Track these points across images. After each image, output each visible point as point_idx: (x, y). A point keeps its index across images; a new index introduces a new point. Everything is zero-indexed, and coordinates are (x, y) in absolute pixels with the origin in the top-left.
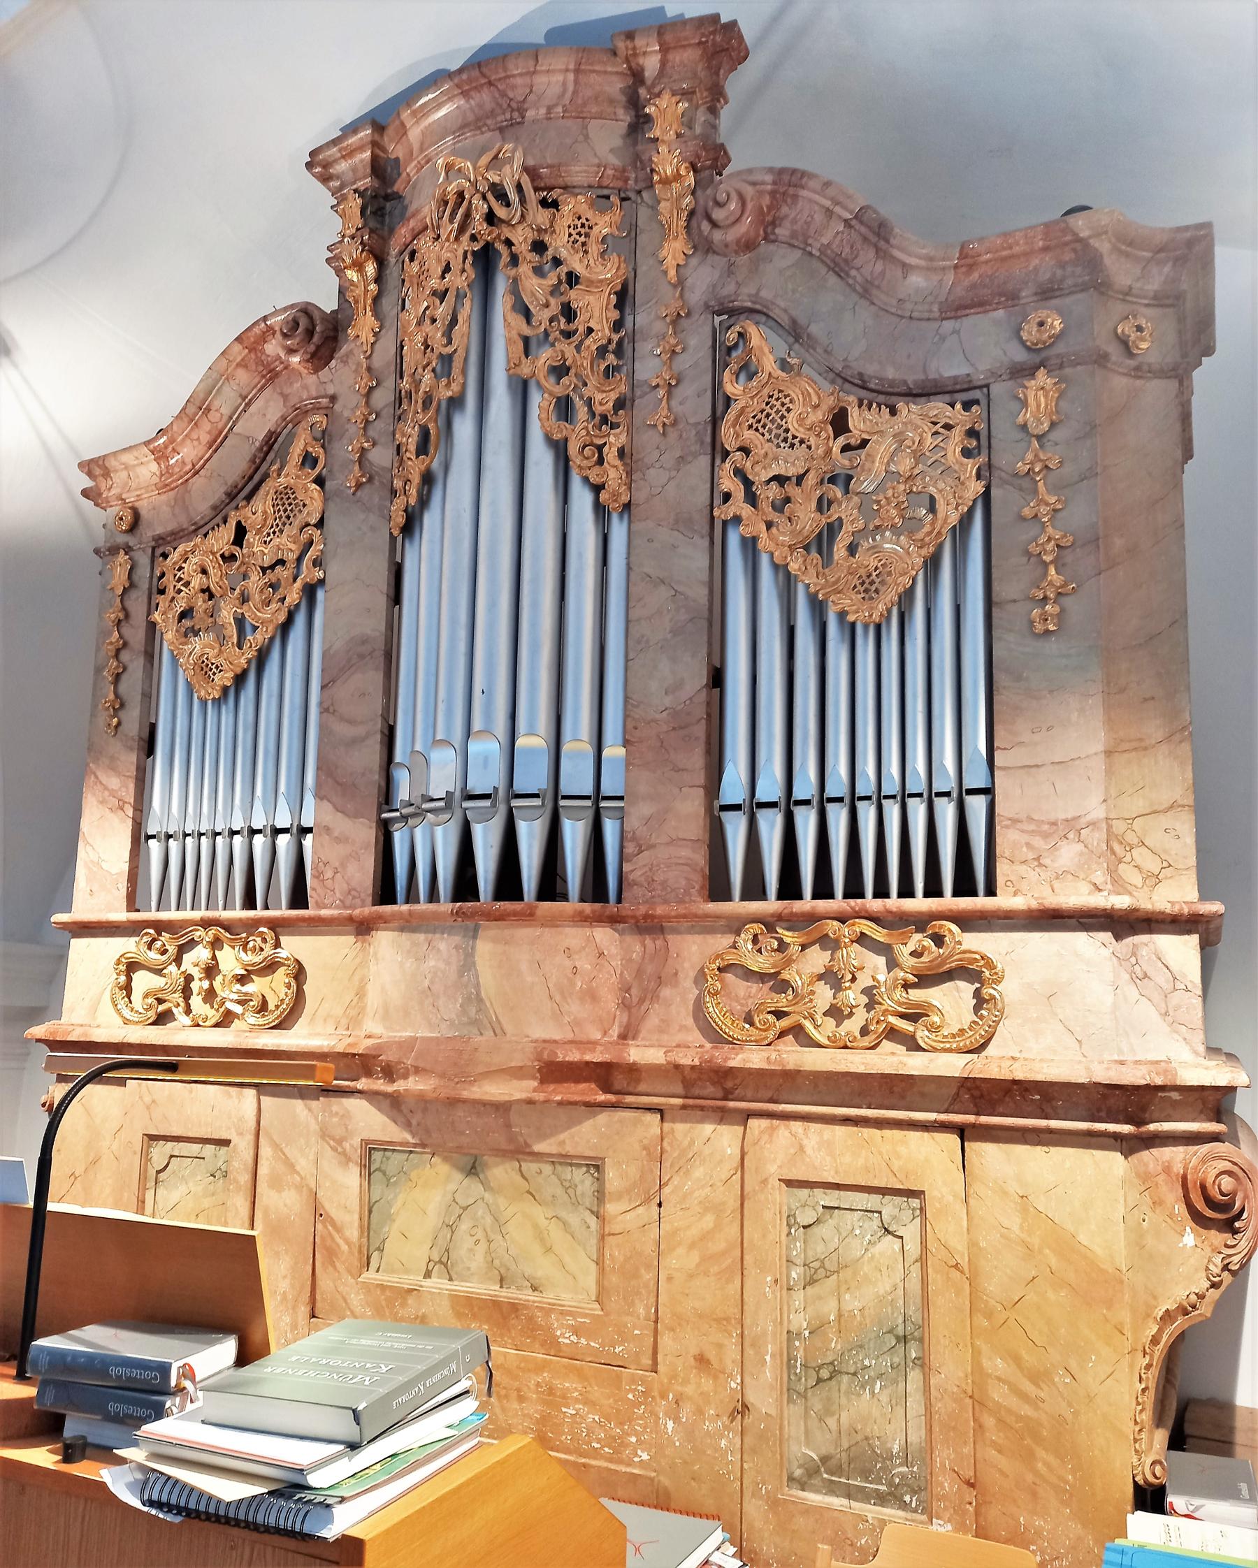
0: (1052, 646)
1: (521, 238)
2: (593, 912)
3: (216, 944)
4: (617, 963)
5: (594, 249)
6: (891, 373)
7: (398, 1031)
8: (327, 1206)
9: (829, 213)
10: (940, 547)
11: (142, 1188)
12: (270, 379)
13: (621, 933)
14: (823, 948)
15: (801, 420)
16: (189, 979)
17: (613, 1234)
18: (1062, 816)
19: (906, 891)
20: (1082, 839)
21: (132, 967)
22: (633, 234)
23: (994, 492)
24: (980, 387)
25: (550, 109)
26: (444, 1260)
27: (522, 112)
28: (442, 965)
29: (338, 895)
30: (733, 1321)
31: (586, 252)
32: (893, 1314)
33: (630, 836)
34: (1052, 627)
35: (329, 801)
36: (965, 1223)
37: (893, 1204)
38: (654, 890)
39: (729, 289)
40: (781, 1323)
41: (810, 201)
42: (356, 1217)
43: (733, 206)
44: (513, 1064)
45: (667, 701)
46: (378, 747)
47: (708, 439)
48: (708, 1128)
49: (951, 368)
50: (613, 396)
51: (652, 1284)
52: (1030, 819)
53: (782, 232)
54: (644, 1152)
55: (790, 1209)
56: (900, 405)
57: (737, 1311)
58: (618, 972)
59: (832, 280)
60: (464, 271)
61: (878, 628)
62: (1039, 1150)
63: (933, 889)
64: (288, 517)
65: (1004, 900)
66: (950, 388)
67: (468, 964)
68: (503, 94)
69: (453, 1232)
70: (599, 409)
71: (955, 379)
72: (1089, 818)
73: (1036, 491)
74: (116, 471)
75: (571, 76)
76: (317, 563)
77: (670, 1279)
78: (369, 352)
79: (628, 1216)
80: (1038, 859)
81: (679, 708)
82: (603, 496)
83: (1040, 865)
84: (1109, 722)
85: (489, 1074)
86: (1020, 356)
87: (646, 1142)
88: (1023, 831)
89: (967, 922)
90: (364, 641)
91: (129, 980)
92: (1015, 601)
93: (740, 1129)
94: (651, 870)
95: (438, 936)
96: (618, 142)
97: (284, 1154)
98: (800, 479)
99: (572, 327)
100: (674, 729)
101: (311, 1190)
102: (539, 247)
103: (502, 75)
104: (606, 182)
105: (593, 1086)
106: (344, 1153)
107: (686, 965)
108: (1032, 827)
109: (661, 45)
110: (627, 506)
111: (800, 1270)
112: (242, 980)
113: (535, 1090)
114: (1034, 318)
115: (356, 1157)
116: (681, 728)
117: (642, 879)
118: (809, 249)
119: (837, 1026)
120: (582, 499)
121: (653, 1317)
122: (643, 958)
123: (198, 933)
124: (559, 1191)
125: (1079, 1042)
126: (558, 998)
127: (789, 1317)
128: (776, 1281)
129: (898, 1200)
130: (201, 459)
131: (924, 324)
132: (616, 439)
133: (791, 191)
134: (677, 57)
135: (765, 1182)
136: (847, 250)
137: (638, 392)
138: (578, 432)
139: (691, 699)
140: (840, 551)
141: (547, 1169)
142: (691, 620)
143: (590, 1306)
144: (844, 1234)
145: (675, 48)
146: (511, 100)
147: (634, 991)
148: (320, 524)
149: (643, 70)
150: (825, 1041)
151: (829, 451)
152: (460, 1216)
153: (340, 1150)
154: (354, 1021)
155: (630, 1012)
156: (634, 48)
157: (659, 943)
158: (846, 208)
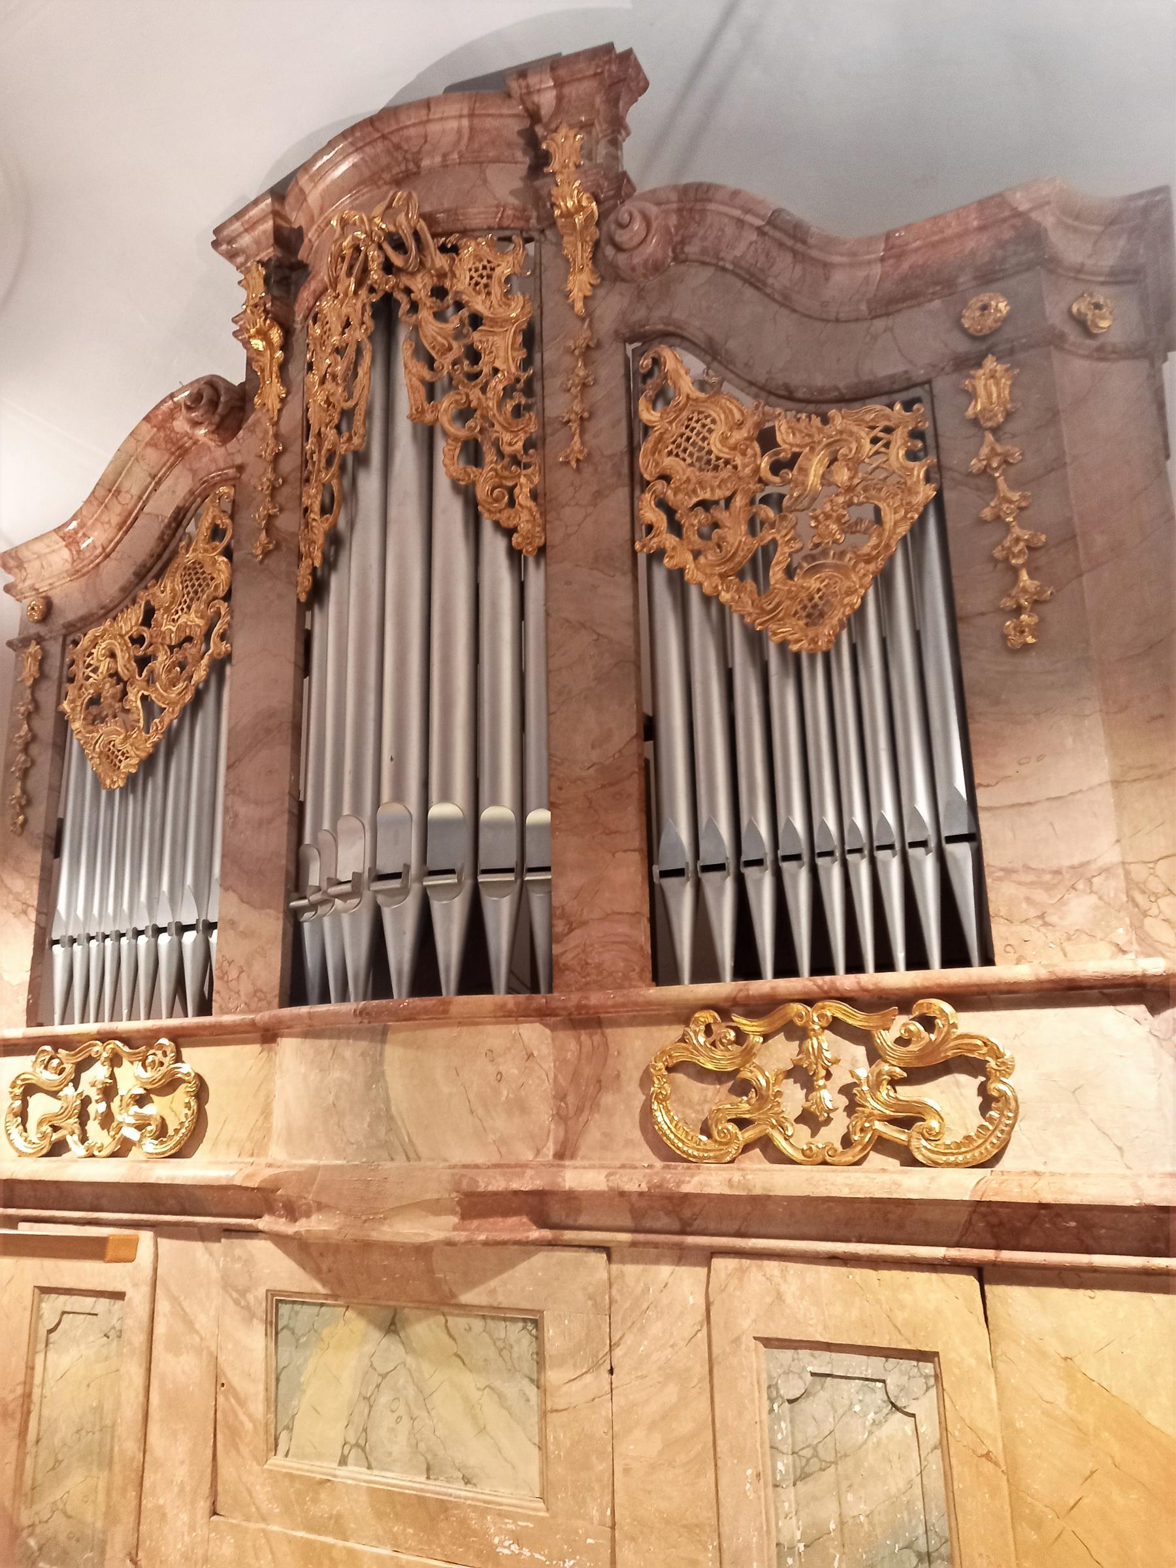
0: (1031, 662)
1: (421, 285)
2: (517, 1004)
3: (115, 1060)
4: (549, 1065)
5: (496, 290)
6: (819, 381)
7: (301, 1158)
8: (229, 1373)
10: (891, 559)
11: (32, 1352)
12: (179, 456)
13: (553, 1028)
14: (789, 1038)
15: (724, 439)
16: (86, 1101)
17: (557, 1411)
18: (1066, 863)
19: (885, 963)
20: (1095, 888)
21: (30, 1089)
22: (538, 272)
23: (948, 496)
24: (921, 384)
25: (445, 156)
26: (362, 1442)
28: (347, 1077)
29: (243, 998)
30: (708, 1529)
31: (489, 294)
32: (910, 1521)
33: (558, 912)
35: (234, 891)
36: (994, 1396)
37: (900, 1370)
38: (588, 975)
39: (641, 313)
40: (768, 1532)
41: (719, 213)
42: (261, 1387)
43: (637, 226)
44: (428, 1197)
45: (595, 756)
46: (285, 828)
47: (625, 470)
48: (665, 1271)
51: (608, 1475)
52: (1027, 868)
53: (692, 250)
54: (590, 1303)
55: (770, 1377)
56: (833, 412)
57: (712, 1514)
58: (551, 1076)
59: (749, 292)
60: (363, 323)
61: (827, 657)
62: (1082, 1294)
64: (196, 592)
65: (1005, 971)
66: (886, 389)
67: (376, 1076)
68: (398, 147)
69: (371, 1407)
70: (507, 450)
71: (892, 378)
72: (1101, 863)
73: (994, 489)
74: (29, 561)
75: (465, 122)
76: (223, 637)
77: (627, 1470)
78: (275, 419)
79: (575, 1386)
80: (1042, 916)
81: (607, 763)
82: (516, 539)
83: (1046, 924)
85: (402, 1210)
86: (962, 346)
87: (591, 1289)
88: (1020, 883)
89: (964, 999)
90: (272, 714)
91: (25, 1104)
92: (983, 614)
93: (706, 1269)
94: (583, 951)
95: (342, 1041)
96: (518, 184)
97: (183, 1309)
99: (476, 368)
100: (603, 786)
101: (211, 1353)
103: (395, 127)
104: (506, 223)
105: (525, 1219)
106: (248, 1308)
107: (630, 1064)
108: (1031, 877)
109: (554, 80)
110: (542, 551)
111: (789, 1459)
112: (141, 1101)
113: (455, 1228)
114: (975, 302)
115: (260, 1310)
116: (611, 784)
117: (575, 962)
118: (721, 263)
119: (813, 1135)
120: (495, 547)
121: (609, 1522)
122: (579, 1059)
123: (96, 1049)
124: (492, 1353)
125: (1120, 1149)
126: (480, 1111)
127: (777, 1524)
128: (758, 1475)
129: (906, 1364)
130: (111, 541)
131: (853, 326)
133: (698, 206)
134: (571, 91)
135: (737, 1341)
136: (762, 258)
137: (549, 430)
139: (620, 751)
140: (776, 574)
141: (478, 1324)
142: (616, 665)
143: (533, 1505)
144: (841, 1411)
145: (569, 82)
146: (406, 152)
147: (570, 1099)
148: (227, 597)
149: (538, 107)
150: (798, 1156)
151: (757, 469)
152: (378, 1386)
153: (243, 1303)
154: (258, 1147)
155: (566, 1125)
156: (528, 86)
157: (597, 1038)
158: (757, 215)
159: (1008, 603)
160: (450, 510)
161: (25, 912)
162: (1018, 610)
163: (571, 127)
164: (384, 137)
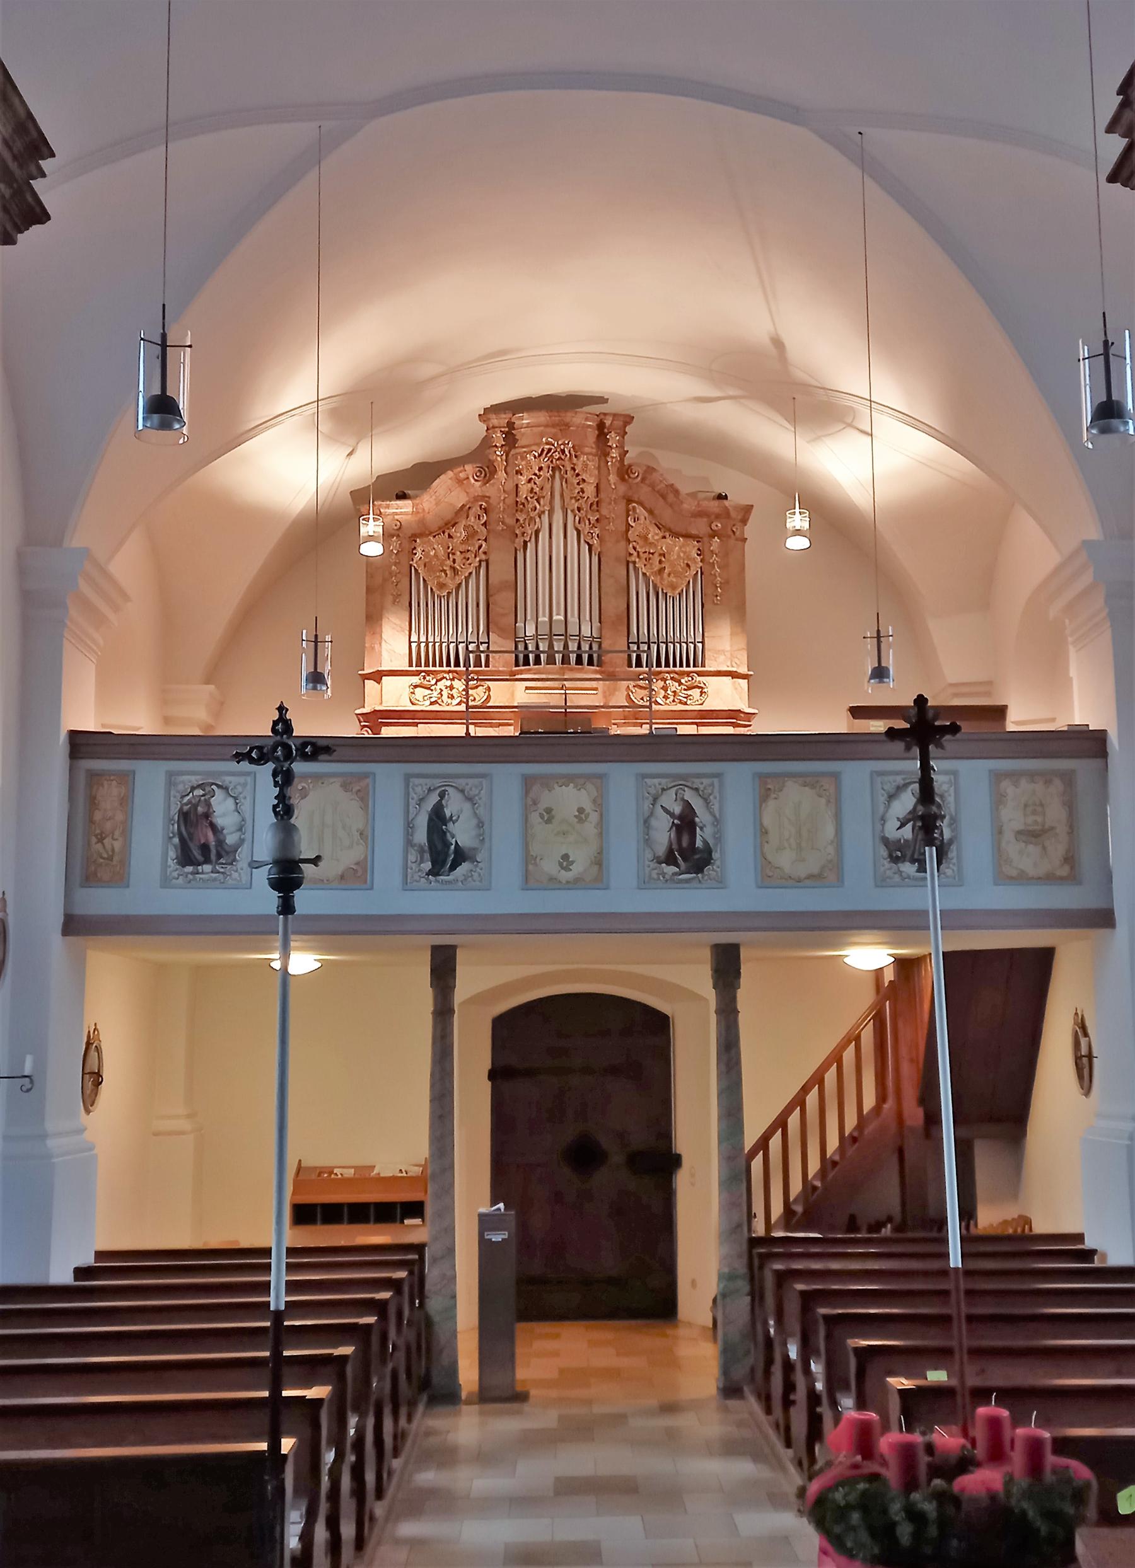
9: (661, 481)
15: (653, 536)
16: (442, 690)
19: (681, 666)
21: (416, 687)
27: (569, 427)
34: (719, 602)
39: (630, 494)
47: (625, 537)
49: (694, 532)
50: (596, 518)
53: (647, 482)
59: (661, 499)
63: (688, 665)
65: (707, 669)
70: (592, 522)
76: (485, 553)
84: (731, 628)
89: (700, 674)
90: (507, 582)
96: (594, 440)
98: (653, 554)
99: (584, 495)
102: (574, 469)
114: (714, 524)
138: (585, 528)
140: (665, 575)
159: (715, 594)
160: (572, 534)
161: (403, 631)
162: (717, 596)
163: (615, 433)
164: (559, 416)
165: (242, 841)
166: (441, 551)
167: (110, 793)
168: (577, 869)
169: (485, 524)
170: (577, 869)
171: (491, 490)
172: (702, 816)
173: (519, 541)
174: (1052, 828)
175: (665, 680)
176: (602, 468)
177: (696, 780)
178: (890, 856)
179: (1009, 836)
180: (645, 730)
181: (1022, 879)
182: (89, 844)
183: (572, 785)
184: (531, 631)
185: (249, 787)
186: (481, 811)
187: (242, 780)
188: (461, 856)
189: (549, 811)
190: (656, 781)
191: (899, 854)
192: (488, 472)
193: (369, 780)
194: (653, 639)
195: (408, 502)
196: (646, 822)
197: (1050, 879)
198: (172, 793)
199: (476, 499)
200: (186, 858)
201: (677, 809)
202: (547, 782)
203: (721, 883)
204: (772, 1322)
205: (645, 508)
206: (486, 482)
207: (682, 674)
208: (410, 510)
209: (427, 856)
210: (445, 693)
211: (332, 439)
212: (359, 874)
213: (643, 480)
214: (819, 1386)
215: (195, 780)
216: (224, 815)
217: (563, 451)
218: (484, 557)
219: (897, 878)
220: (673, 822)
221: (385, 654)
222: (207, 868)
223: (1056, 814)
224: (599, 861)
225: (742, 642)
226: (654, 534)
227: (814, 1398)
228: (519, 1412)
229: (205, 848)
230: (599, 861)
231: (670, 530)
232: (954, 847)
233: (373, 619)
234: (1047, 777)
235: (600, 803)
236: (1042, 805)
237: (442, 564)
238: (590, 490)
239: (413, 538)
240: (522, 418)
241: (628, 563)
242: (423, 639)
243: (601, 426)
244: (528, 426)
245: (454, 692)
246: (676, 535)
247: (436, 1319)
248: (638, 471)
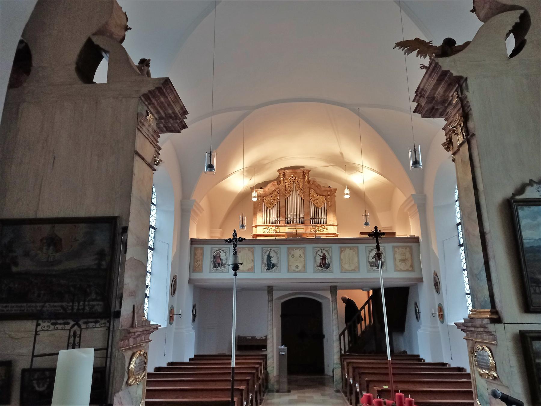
19: (322, 223)
21: (264, 229)
49: (324, 194)
53: (314, 184)
65: (327, 224)
89: (326, 225)
102: (298, 182)
132: (303, 195)
134: (307, 172)
138: (300, 194)
160: (297, 195)
165: (227, 262)
166: (269, 199)
167: (199, 252)
168: (300, 268)
169: (279, 194)
170: (300, 268)
171: (280, 186)
172: (327, 256)
173: (286, 197)
174: (408, 259)
175: (318, 227)
176: (304, 181)
177: (326, 248)
178: (370, 265)
179: (397, 261)
180: (314, 237)
181: (401, 271)
182: (194, 263)
183: (298, 249)
184: (289, 216)
185: (228, 250)
186: (278, 255)
187: (227, 249)
188: (274, 265)
189: (293, 255)
190: (317, 248)
191: (372, 265)
192: (279, 183)
193: (254, 249)
194: (316, 218)
195: (263, 189)
196: (315, 258)
197: (407, 270)
198: (212, 251)
199: (277, 188)
200: (215, 266)
201: (322, 255)
202: (293, 249)
203: (332, 271)
204: (346, 375)
205: (313, 190)
206: (279, 184)
207: (322, 225)
208: (263, 191)
209: (267, 265)
210: (271, 230)
211: (246, 176)
212: (252, 269)
213: (313, 184)
214: (358, 390)
215: (217, 249)
216: (223, 257)
217: (295, 178)
218: (279, 201)
219: (372, 270)
220: (321, 258)
221: (258, 222)
222: (219, 268)
223: (408, 255)
224: (304, 267)
225: (335, 218)
226: (315, 195)
227: (357, 393)
228: (288, 395)
229: (219, 264)
230: (304, 267)
231: (319, 194)
232: (385, 263)
233: (255, 214)
234: (406, 247)
235: (304, 253)
236: (405, 254)
237: (270, 202)
238: (301, 186)
239: (263, 197)
240: (287, 171)
241: (310, 201)
242: (266, 218)
243: (303, 172)
244: (288, 173)
245: (272, 230)
246: (320, 195)
247: (269, 372)
248: (311, 182)
